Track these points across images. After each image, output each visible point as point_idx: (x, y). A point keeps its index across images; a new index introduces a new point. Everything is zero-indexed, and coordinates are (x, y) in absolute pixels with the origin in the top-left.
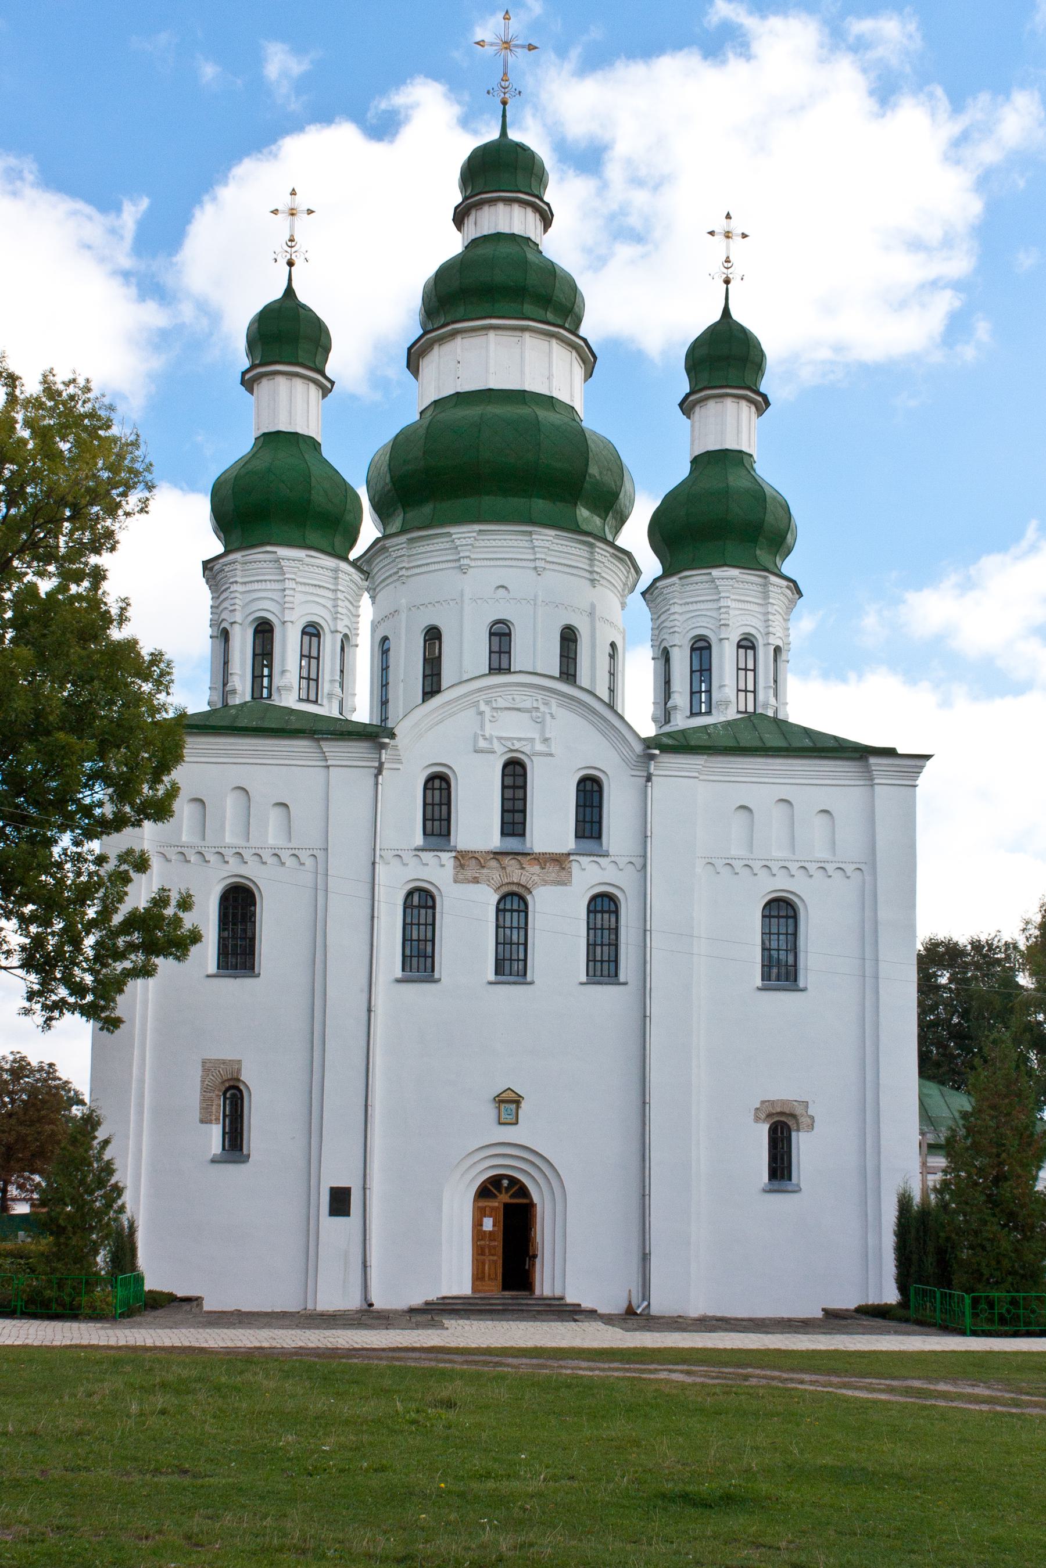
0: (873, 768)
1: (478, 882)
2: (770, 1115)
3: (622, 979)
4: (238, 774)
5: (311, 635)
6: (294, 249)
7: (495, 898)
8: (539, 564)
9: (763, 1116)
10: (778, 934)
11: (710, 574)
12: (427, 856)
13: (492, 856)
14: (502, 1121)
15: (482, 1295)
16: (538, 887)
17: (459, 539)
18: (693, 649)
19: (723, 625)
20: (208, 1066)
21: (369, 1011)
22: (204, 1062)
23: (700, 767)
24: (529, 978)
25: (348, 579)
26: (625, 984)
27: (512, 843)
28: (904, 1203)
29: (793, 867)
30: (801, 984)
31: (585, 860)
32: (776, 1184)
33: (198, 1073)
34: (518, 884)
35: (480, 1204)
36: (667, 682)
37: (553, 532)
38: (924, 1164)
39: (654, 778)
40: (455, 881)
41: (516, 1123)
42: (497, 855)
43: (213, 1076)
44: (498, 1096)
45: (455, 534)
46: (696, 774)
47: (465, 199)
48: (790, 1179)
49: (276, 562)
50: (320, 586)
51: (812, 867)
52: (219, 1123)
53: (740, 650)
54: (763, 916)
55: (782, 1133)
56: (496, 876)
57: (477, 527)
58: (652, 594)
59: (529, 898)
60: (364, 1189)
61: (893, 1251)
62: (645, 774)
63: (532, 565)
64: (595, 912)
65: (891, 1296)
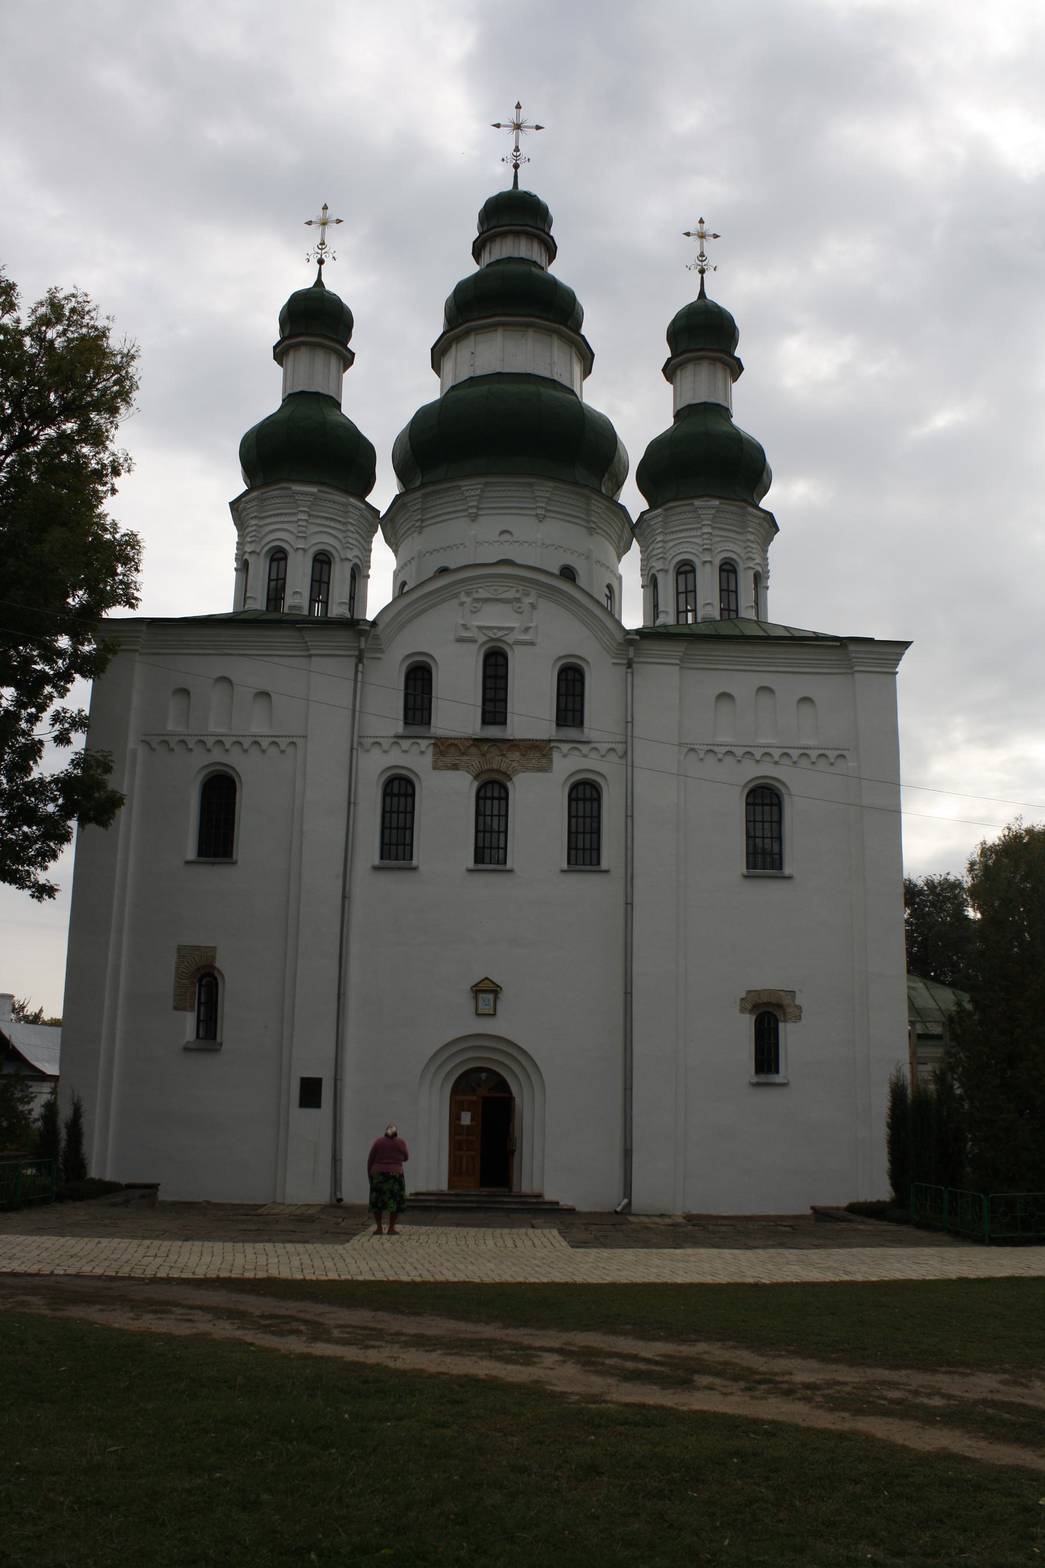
0: (853, 655)
1: (457, 769)
3: (604, 865)
4: (219, 666)
6: (323, 251)
7: (476, 785)
8: (539, 511)
9: (749, 1007)
10: (763, 822)
11: (692, 504)
12: (406, 744)
13: (471, 742)
14: (480, 1012)
15: (458, 1191)
16: (518, 774)
17: (467, 490)
18: (678, 573)
19: (706, 549)
20: (184, 952)
21: (344, 897)
22: (180, 948)
23: (681, 654)
24: (509, 866)
25: (358, 513)
26: (607, 871)
27: (494, 732)
28: (897, 1093)
29: (776, 753)
30: (787, 870)
31: (565, 748)
32: (763, 1078)
33: (172, 960)
34: (498, 771)
35: (458, 1098)
36: (656, 606)
37: (552, 484)
38: (913, 1054)
39: (634, 665)
40: (435, 768)
41: (494, 1015)
42: (478, 742)
43: (188, 963)
44: (475, 986)
45: (464, 486)
46: (677, 662)
47: (481, 234)
48: (777, 1072)
49: (291, 497)
50: (331, 519)
51: (795, 754)
52: (194, 1010)
53: (723, 573)
54: (747, 804)
55: (769, 1024)
56: (476, 762)
57: (483, 480)
58: (640, 528)
59: (509, 785)
60: (336, 1080)
61: (886, 1145)
62: (625, 662)
63: (534, 513)
64: (577, 799)
65: (882, 1191)
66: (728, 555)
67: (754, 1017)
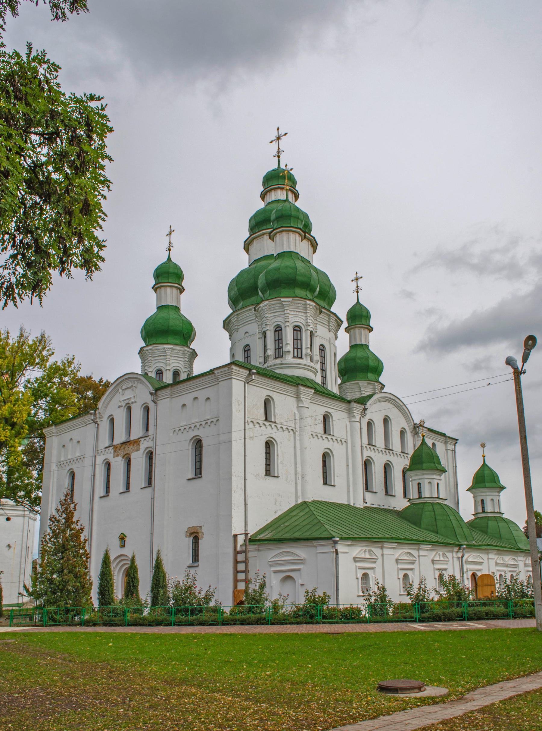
2: (191, 534)
5: (160, 373)
7: (123, 460)
9: (188, 534)
39: (158, 402)
50: (161, 356)
63: (254, 321)
66: (276, 323)
67: (192, 538)
